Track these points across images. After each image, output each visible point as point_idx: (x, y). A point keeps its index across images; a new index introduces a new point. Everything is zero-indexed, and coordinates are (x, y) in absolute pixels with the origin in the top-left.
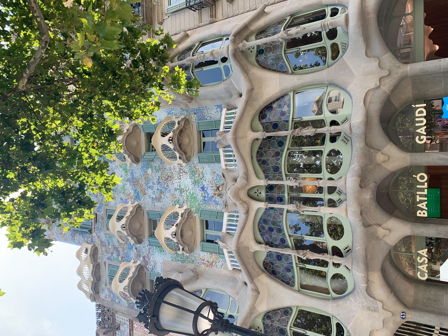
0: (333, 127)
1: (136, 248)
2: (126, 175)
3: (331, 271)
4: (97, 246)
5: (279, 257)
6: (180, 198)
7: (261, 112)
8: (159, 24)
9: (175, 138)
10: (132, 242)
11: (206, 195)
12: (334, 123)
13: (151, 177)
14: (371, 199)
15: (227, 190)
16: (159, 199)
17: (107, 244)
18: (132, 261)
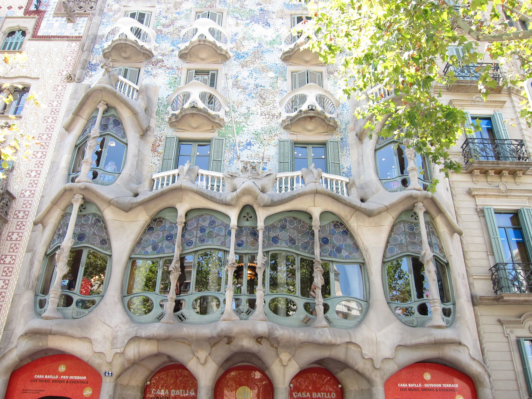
0: (323, 307)
1: (173, 51)
3: (155, 297)
5: (170, 238)
6: (237, 113)
7: (342, 224)
8: (451, 101)
9: (313, 113)
10: (182, 46)
12: (326, 308)
13: (264, 76)
14: (242, 346)
15: (252, 180)
16: (236, 85)
17: (178, 11)
18: (157, 45)
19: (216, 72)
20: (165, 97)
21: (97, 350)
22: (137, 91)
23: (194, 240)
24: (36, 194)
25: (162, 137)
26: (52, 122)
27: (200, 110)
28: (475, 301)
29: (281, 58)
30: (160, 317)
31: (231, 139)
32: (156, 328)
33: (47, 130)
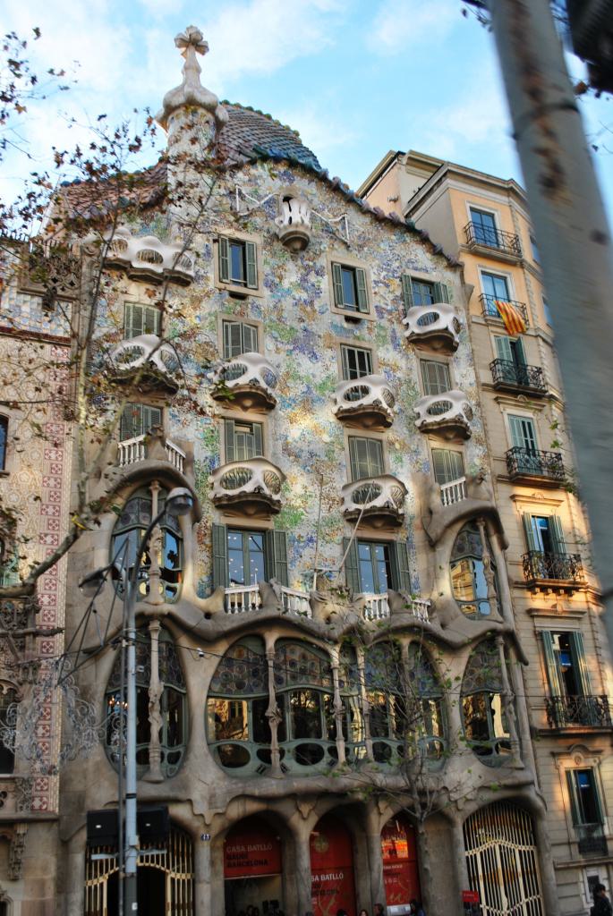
2: (316, 386)
4: (192, 286)
11: (302, 544)
17: (198, 313)
19: (259, 426)
20: (202, 460)
21: (197, 812)
22: (184, 459)
23: (283, 676)
24: (59, 600)
25: (207, 522)
26: (55, 486)
27: (264, 497)
28: (535, 733)
29: (336, 415)
30: (261, 772)
31: (289, 532)
32: (275, 787)
33: (52, 499)
